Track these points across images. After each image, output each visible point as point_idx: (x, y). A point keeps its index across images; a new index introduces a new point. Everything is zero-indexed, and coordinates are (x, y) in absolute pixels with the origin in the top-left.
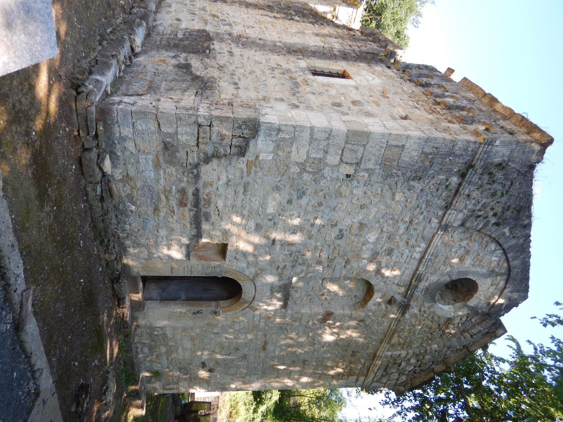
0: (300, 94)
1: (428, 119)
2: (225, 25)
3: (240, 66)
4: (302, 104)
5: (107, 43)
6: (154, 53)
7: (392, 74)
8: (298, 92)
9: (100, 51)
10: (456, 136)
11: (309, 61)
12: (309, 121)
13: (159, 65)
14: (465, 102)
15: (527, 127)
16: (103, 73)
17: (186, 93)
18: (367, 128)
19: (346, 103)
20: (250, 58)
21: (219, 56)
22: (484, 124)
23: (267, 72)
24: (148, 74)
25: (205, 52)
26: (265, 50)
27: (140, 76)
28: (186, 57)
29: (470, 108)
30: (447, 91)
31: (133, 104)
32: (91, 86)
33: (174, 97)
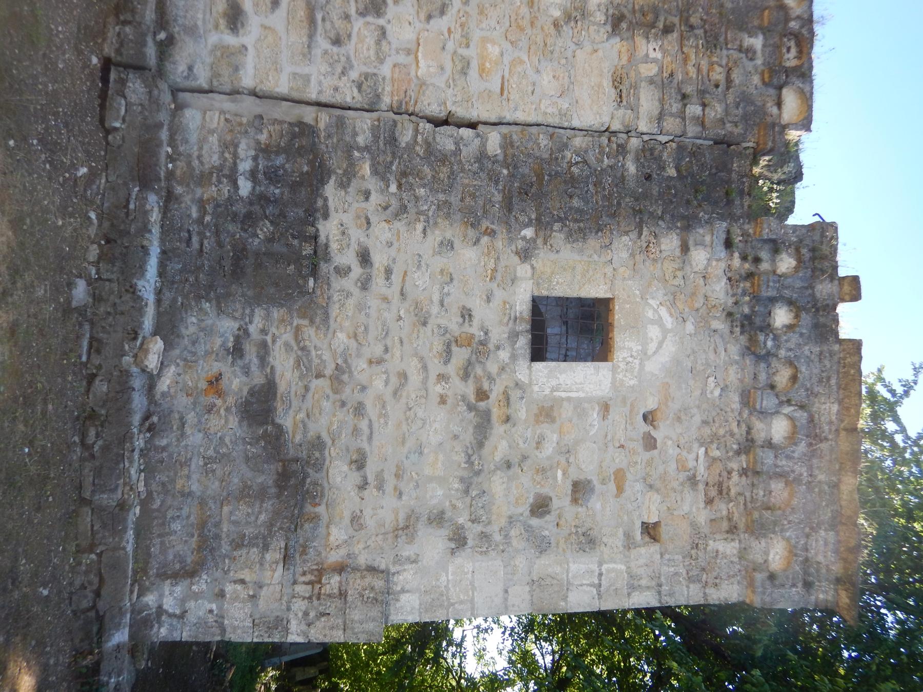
0: (480, 479)
1: (694, 525)
2: (362, 14)
3: (378, 350)
4: (475, 525)
5: (98, 435)
6: (190, 325)
7: (719, 290)
8: (478, 473)
9: (93, 492)
10: (711, 591)
11: (543, 259)
12: (472, 601)
13: (210, 409)
14: (802, 447)
15: (845, 568)
16: (121, 609)
17: (268, 556)
18: (565, 599)
19: (561, 502)
20: (408, 288)
21: (337, 283)
22: (788, 540)
23: (436, 366)
24: (193, 466)
25: (303, 292)
26: (448, 216)
27: (179, 484)
28: (264, 331)
29: (794, 479)
30: (789, 402)
31: (182, 616)
32: (112, 680)
33: (246, 575)
